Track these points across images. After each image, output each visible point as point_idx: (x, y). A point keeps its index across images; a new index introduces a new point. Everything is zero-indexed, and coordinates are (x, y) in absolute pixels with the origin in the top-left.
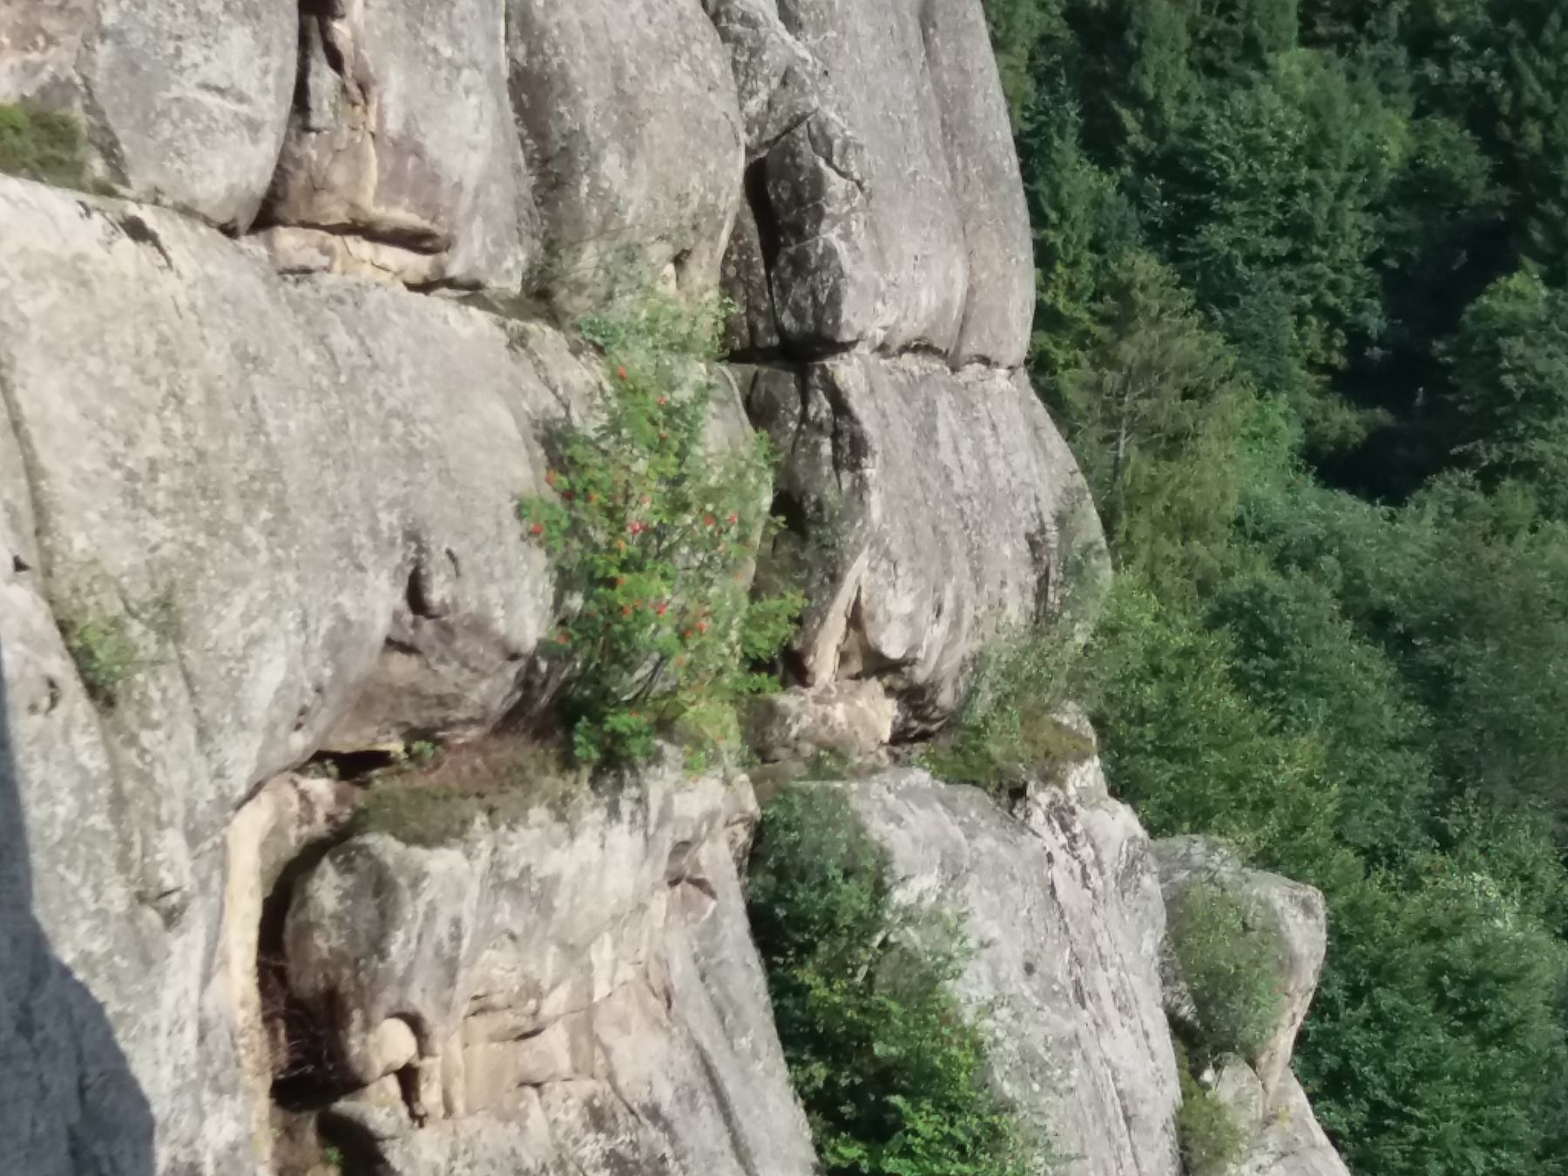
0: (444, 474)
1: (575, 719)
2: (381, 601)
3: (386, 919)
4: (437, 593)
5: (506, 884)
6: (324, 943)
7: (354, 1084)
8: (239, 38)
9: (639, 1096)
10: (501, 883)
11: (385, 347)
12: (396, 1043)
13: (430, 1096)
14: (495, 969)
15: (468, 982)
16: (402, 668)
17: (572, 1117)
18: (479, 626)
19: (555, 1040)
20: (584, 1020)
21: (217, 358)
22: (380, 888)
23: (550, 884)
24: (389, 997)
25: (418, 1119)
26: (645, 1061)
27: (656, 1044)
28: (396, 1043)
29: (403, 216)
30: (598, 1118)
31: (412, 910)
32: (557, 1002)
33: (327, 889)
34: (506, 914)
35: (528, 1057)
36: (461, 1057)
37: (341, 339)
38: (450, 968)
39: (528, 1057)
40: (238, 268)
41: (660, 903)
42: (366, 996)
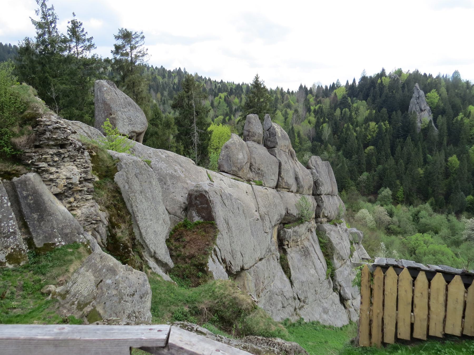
3: (285, 234)
4: (289, 212)
6: (282, 236)
7: (284, 245)
13: (290, 246)
16: (287, 217)
18: (292, 214)
22: (285, 232)
23: (298, 232)
25: (288, 248)
28: (287, 243)
29: (286, 187)
31: (287, 234)
33: (282, 232)
34: (295, 234)
35: (297, 244)
36: (291, 244)
38: (290, 237)
42: (284, 239)
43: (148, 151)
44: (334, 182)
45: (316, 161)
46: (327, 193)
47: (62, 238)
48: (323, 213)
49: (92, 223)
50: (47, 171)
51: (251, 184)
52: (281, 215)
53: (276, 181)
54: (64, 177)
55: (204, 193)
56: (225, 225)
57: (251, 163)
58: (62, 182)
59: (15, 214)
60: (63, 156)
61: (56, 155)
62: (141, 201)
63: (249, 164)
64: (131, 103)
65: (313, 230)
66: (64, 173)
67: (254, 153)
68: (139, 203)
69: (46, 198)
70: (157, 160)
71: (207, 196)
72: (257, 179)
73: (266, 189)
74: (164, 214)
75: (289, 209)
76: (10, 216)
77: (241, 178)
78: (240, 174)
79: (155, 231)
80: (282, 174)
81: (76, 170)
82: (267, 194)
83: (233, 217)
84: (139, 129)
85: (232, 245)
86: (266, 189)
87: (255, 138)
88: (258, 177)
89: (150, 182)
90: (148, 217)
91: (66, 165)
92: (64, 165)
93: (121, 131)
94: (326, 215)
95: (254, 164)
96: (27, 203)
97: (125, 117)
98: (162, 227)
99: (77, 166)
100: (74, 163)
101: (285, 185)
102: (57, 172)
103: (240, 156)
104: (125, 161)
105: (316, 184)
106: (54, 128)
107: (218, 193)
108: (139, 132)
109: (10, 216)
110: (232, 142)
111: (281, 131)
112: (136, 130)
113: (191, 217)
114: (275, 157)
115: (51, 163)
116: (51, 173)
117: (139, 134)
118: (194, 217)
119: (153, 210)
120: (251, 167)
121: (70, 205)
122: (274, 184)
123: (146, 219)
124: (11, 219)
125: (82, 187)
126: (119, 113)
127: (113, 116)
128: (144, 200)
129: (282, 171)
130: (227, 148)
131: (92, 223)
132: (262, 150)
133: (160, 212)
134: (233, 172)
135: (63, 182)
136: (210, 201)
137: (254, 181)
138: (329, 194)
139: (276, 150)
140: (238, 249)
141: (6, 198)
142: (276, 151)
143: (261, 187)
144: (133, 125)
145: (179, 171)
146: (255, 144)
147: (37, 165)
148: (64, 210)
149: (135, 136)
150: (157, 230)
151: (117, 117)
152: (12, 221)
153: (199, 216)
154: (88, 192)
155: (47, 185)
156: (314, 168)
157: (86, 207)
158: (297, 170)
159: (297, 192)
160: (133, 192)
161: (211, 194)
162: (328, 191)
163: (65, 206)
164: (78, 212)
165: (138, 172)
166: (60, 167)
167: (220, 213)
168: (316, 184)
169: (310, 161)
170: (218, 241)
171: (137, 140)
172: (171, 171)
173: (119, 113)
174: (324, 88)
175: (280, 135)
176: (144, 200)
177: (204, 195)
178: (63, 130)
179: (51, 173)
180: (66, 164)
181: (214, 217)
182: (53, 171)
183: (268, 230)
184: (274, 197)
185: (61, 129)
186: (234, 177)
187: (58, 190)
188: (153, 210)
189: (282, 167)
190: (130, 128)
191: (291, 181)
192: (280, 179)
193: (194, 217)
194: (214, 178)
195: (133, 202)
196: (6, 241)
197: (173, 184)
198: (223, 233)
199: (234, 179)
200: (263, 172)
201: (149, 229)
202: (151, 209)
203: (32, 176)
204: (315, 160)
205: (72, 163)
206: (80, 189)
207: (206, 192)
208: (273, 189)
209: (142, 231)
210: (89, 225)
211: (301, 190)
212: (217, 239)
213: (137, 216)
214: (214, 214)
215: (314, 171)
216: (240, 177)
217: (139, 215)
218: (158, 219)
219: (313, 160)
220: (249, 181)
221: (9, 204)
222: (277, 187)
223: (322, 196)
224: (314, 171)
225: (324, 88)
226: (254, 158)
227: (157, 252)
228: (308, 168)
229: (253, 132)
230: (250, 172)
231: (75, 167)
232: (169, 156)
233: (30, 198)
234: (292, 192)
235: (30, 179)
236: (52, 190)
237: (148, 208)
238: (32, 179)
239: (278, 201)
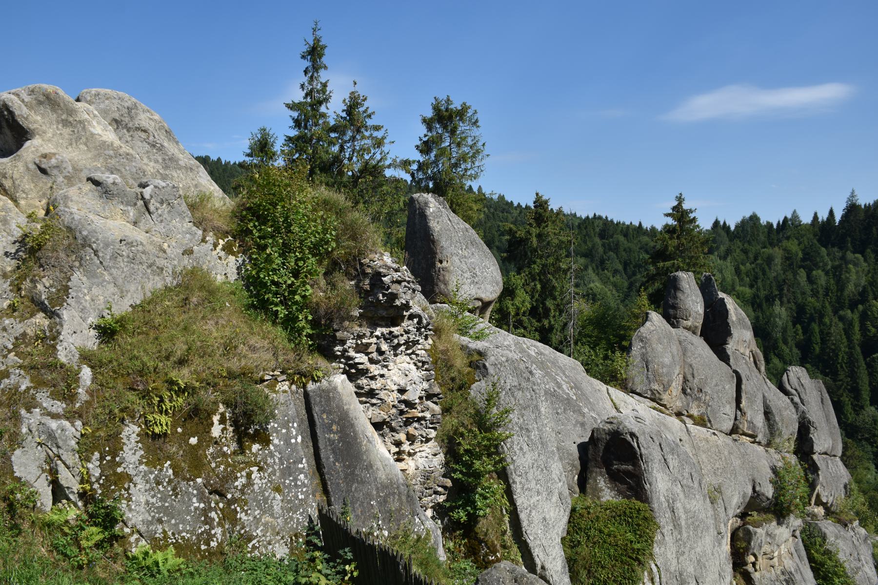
0: (758, 471)
1: (779, 510)
2: (750, 491)
4: (757, 489)
5: (768, 534)
7: (746, 564)
8: (728, 406)
9: (788, 570)
10: (768, 534)
11: (748, 452)
12: (751, 559)
13: (758, 567)
14: (766, 548)
15: (763, 550)
17: (779, 572)
19: (776, 560)
20: (780, 556)
21: (726, 453)
23: (775, 535)
24: (751, 551)
25: (756, 571)
26: (789, 564)
27: (791, 562)
30: (783, 573)
31: (755, 538)
32: (776, 554)
34: (768, 540)
36: (762, 562)
37: (742, 451)
38: (761, 547)
39: (771, 562)
40: (728, 440)
41: (791, 539)
43: (505, 340)
44: (835, 427)
45: (799, 378)
46: (823, 451)
47: (383, 520)
48: (818, 496)
49: (436, 493)
50: (364, 372)
51: (685, 423)
52: (744, 496)
53: (733, 417)
54: (395, 388)
55: (629, 438)
56: (668, 514)
57: (684, 377)
58: (392, 398)
59: (308, 462)
60: (396, 341)
61: (385, 339)
62: (521, 449)
64: (475, 240)
65: (798, 533)
66: (395, 378)
67: (689, 354)
69: (359, 429)
71: (635, 445)
72: (695, 412)
73: (714, 434)
75: (758, 481)
76: (300, 466)
77: (666, 408)
78: (665, 397)
79: (544, 519)
80: (744, 404)
81: (416, 374)
83: (682, 496)
84: (488, 294)
85: (681, 558)
86: (714, 434)
87: (689, 323)
88: (698, 407)
89: (536, 407)
90: (533, 484)
91: (398, 361)
92: (395, 362)
94: (825, 501)
95: (689, 377)
96: (329, 439)
97: (465, 267)
98: (557, 510)
99: (415, 364)
100: (411, 359)
101: (749, 428)
102: (382, 376)
103: (667, 360)
104: (492, 358)
105: (804, 429)
106: (393, 282)
107: (655, 439)
109: (300, 466)
110: (652, 328)
111: (736, 309)
112: (483, 296)
113: (597, 491)
115: (375, 355)
116: (373, 378)
117: (486, 305)
118: (601, 490)
119: (542, 470)
121: (397, 450)
122: (728, 425)
123: (530, 490)
124: (301, 471)
125: (423, 411)
126: (456, 259)
127: (444, 264)
128: (525, 448)
129: (743, 395)
130: (642, 341)
131: (436, 493)
132: (701, 349)
133: (554, 476)
134: (653, 393)
135: (391, 398)
136: (641, 455)
137: (690, 416)
138: (826, 453)
140: (691, 569)
141: (295, 425)
142: (729, 352)
143: (704, 430)
144: (477, 286)
145: (564, 387)
146: (688, 334)
147: (352, 359)
148: (389, 459)
150: (547, 517)
151: (452, 268)
152: (302, 476)
153: (612, 489)
154: (432, 424)
155: (361, 402)
156: (794, 392)
157: (424, 454)
159: (769, 445)
161: (641, 439)
162: (826, 446)
163: (389, 451)
164: (410, 465)
165: (516, 384)
166: (386, 367)
167: (660, 483)
168: (804, 429)
169: (785, 377)
170: (656, 550)
172: (551, 386)
173: (456, 259)
175: (734, 319)
176: (525, 448)
177: (629, 443)
178: (405, 287)
179: (373, 378)
180: (399, 359)
181: (649, 492)
182: (376, 373)
183: (723, 530)
184: (730, 453)
185: (403, 284)
186: (655, 404)
187: (384, 416)
188: (542, 470)
189: (743, 387)
191: (759, 420)
193: (601, 490)
194: (623, 404)
195: (505, 449)
196: (292, 518)
197: (558, 413)
198: (665, 531)
199: (654, 408)
200: (708, 397)
201: (533, 514)
202: (538, 467)
203: (340, 380)
205: (407, 359)
206: (420, 415)
207: (633, 435)
209: (523, 516)
210: (430, 496)
211: (777, 440)
212: (655, 545)
213: (514, 482)
214: (647, 486)
215: (796, 399)
216: (664, 406)
217: (518, 479)
218: (550, 493)
219: (791, 374)
220: (679, 414)
221: (299, 439)
222: (734, 430)
223: (815, 457)
224: (796, 399)
226: (691, 366)
227: (547, 566)
229: (686, 310)
231: (413, 367)
232: (540, 353)
233: (334, 427)
234: (759, 443)
235: (335, 388)
236: (370, 413)
237: (533, 464)
238: (340, 389)
239: (737, 463)
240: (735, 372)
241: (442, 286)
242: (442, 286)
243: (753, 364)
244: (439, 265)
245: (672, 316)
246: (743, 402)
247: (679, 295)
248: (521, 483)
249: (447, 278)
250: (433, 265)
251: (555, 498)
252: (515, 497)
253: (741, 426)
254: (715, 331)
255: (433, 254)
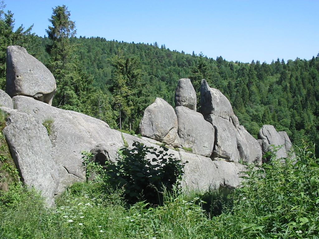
55: (104, 153)
62: (28, 155)
63: (175, 130)
68: (25, 156)
70: (61, 120)
71: (107, 156)
74: (52, 169)
75: (226, 179)
82: (197, 162)
88: (188, 144)
93: (26, 92)
95: (183, 129)
108: (45, 93)
114: (212, 124)
120: (180, 133)
127: (20, 77)
128: (30, 154)
130: (149, 112)
139: (213, 117)
144: (40, 87)
146: (187, 110)
149: (45, 98)
158: (240, 138)
160: (19, 146)
171: (46, 102)
174: (43, 37)
176: (30, 154)
177: (105, 155)
190: (37, 90)
192: (216, 147)
204: (268, 129)
207: (105, 151)
208: (207, 157)
213: (23, 169)
215: (266, 141)
217: (25, 168)
225: (43, 37)
228: (259, 137)
230: (179, 138)
240: (215, 127)
241: (19, 88)
242: (19, 88)
243: (232, 124)
244: (17, 78)
245: (175, 102)
246: (219, 141)
247: (181, 90)
248: (26, 169)
249: (21, 84)
250: (14, 78)
251: (49, 176)
252: (23, 175)
253: (218, 153)
254: (205, 107)
255: (14, 73)
